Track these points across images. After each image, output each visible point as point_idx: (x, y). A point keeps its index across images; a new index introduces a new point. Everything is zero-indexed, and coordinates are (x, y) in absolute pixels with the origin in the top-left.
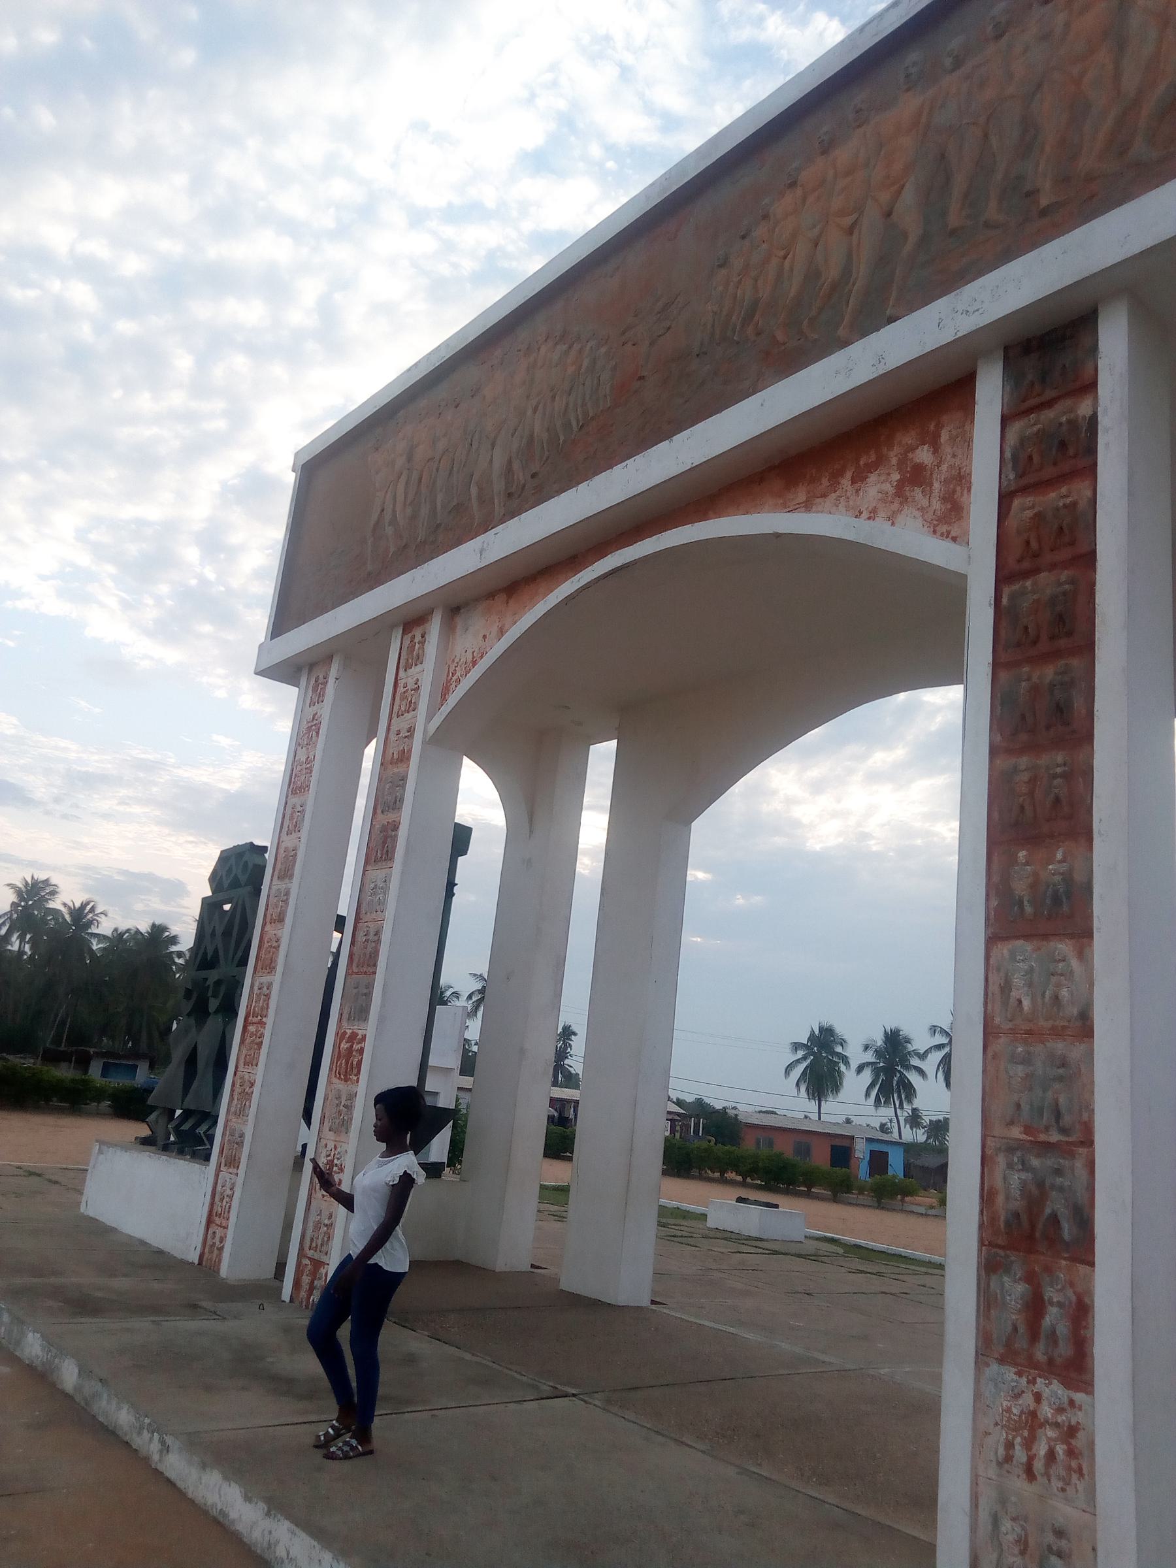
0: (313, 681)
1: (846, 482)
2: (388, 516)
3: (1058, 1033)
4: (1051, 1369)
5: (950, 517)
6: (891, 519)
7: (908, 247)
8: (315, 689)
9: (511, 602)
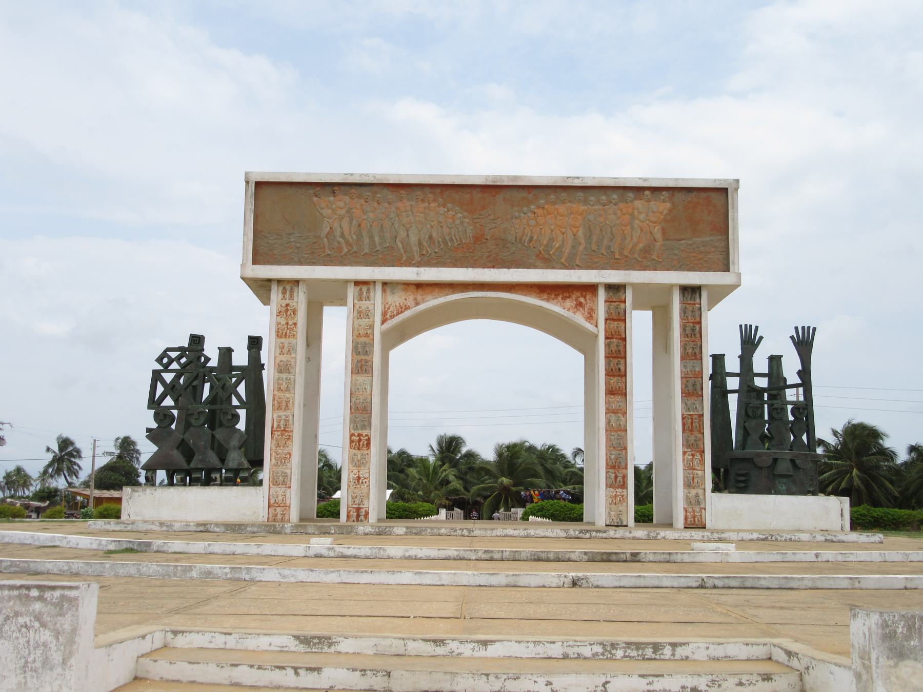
0: (281, 288)
1: (560, 298)
2: (338, 234)
4: (619, 487)
5: (591, 316)
6: (574, 313)
7: (581, 248)
8: (284, 293)
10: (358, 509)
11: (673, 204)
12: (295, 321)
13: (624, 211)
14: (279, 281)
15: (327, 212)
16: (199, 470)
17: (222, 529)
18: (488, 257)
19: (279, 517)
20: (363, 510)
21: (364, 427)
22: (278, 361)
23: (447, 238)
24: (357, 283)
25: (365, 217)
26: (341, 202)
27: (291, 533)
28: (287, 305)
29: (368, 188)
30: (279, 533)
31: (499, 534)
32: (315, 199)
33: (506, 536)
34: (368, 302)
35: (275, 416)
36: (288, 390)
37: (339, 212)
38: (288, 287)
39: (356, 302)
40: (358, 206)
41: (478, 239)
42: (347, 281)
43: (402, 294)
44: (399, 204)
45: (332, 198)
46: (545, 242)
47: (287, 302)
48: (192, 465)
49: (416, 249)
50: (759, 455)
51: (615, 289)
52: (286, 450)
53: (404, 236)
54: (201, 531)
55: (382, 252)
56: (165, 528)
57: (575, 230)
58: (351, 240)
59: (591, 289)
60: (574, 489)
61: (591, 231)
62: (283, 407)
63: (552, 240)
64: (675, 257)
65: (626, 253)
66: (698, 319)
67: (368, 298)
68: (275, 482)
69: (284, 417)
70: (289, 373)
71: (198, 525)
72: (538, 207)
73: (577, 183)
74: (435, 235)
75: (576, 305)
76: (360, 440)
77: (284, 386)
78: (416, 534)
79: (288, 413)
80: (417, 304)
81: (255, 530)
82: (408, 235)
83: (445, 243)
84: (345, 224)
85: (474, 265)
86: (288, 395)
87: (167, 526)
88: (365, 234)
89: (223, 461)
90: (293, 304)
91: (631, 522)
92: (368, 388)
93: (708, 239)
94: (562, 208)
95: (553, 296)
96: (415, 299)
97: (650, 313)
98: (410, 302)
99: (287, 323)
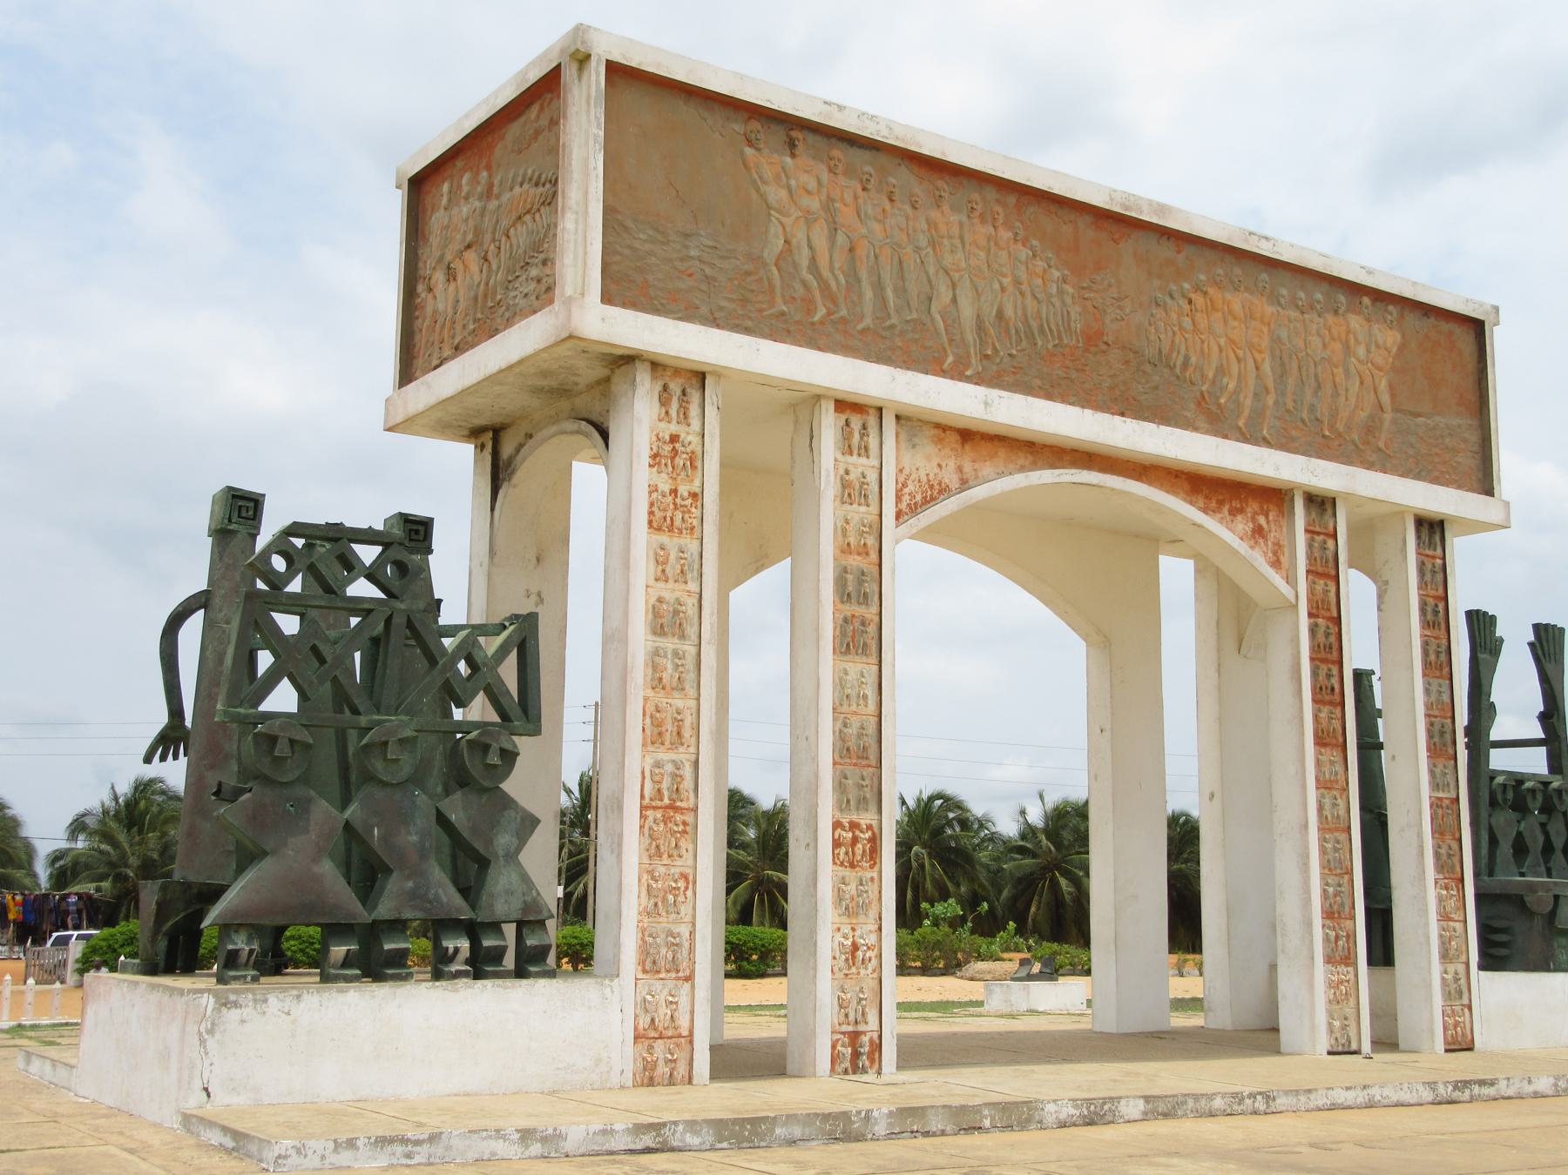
0: (658, 387)
3: (1337, 830)
6: (1252, 547)
7: (1270, 400)
8: (664, 398)
9: (967, 447)
10: (855, 1036)
11: (1403, 336)
12: (695, 487)
13: (1335, 331)
14: (657, 366)
15: (776, 194)
16: (397, 926)
17: (708, 1137)
18: (1112, 388)
19: (663, 1069)
20: (865, 1039)
21: (862, 803)
22: (653, 600)
23: (1034, 324)
24: (844, 405)
25: (864, 231)
26: (807, 172)
27: (891, 1136)
28: (674, 439)
29: (867, 155)
30: (859, 1138)
31: (1320, 1103)
32: (749, 151)
33: (1333, 1107)
34: (863, 460)
35: (649, 761)
36: (680, 687)
37: (805, 201)
38: (676, 388)
39: (840, 457)
40: (848, 197)
41: (1093, 339)
42: (816, 398)
43: (931, 449)
44: (935, 214)
45: (788, 160)
46: (1211, 375)
47: (674, 428)
48: (385, 909)
49: (970, 337)
50: (1531, 887)
51: (1320, 503)
52: (681, 865)
53: (947, 299)
54: (648, 1150)
55: (902, 333)
56: (536, 1148)
57: (1257, 355)
58: (833, 284)
59: (1274, 496)
60: (98, 889)
61: (1282, 364)
62: (667, 737)
63: (1222, 371)
64: (1411, 452)
65: (1340, 427)
66: (1441, 592)
67: (864, 450)
68: (649, 964)
69: (669, 768)
70: (683, 637)
71: (639, 1129)
72: (1197, 289)
73: (1265, 249)
74: (1009, 312)
75: (1253, 531)
76: (855, 840)
77: (668, 675)
78: (1166, 1115)
79: (683, 755)
80: (965, 484)
81: (797, 1132)
82: (954, 300)
83: (1030, 335)
84: (820, 241)
85: (1088, 400)
86: (679, 703)
87: (544, 1140)
88: (864, 275)
89: (468, 892)
90: (690, 437)
91: (1366, 1047)
92: (870, 692)
93: (1456, 421)
94: (1237, 301)
95: (1213, 505)
96: (960, 469)
97: (1191, 563)
98: (950, 477)
99: (674, 492)
